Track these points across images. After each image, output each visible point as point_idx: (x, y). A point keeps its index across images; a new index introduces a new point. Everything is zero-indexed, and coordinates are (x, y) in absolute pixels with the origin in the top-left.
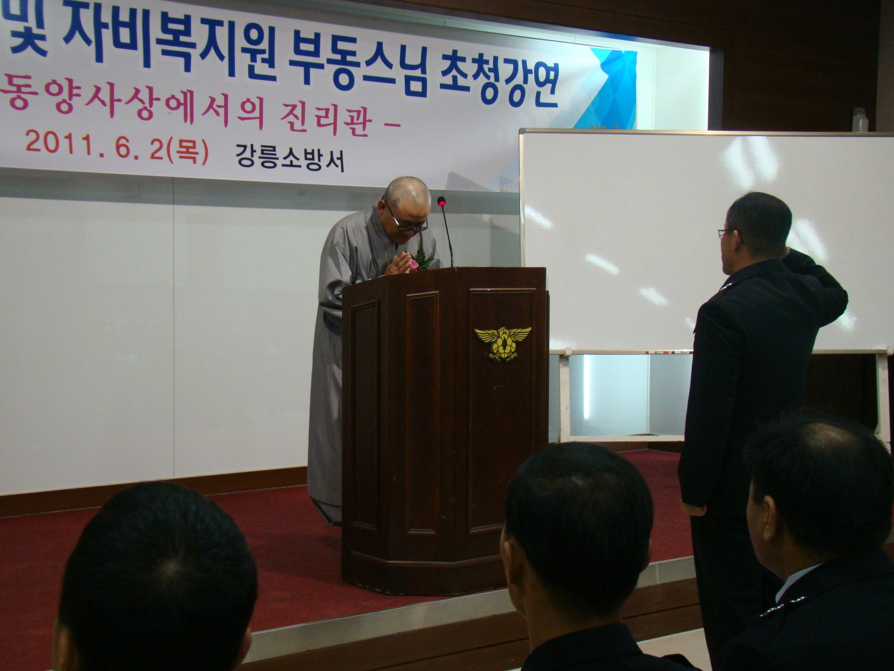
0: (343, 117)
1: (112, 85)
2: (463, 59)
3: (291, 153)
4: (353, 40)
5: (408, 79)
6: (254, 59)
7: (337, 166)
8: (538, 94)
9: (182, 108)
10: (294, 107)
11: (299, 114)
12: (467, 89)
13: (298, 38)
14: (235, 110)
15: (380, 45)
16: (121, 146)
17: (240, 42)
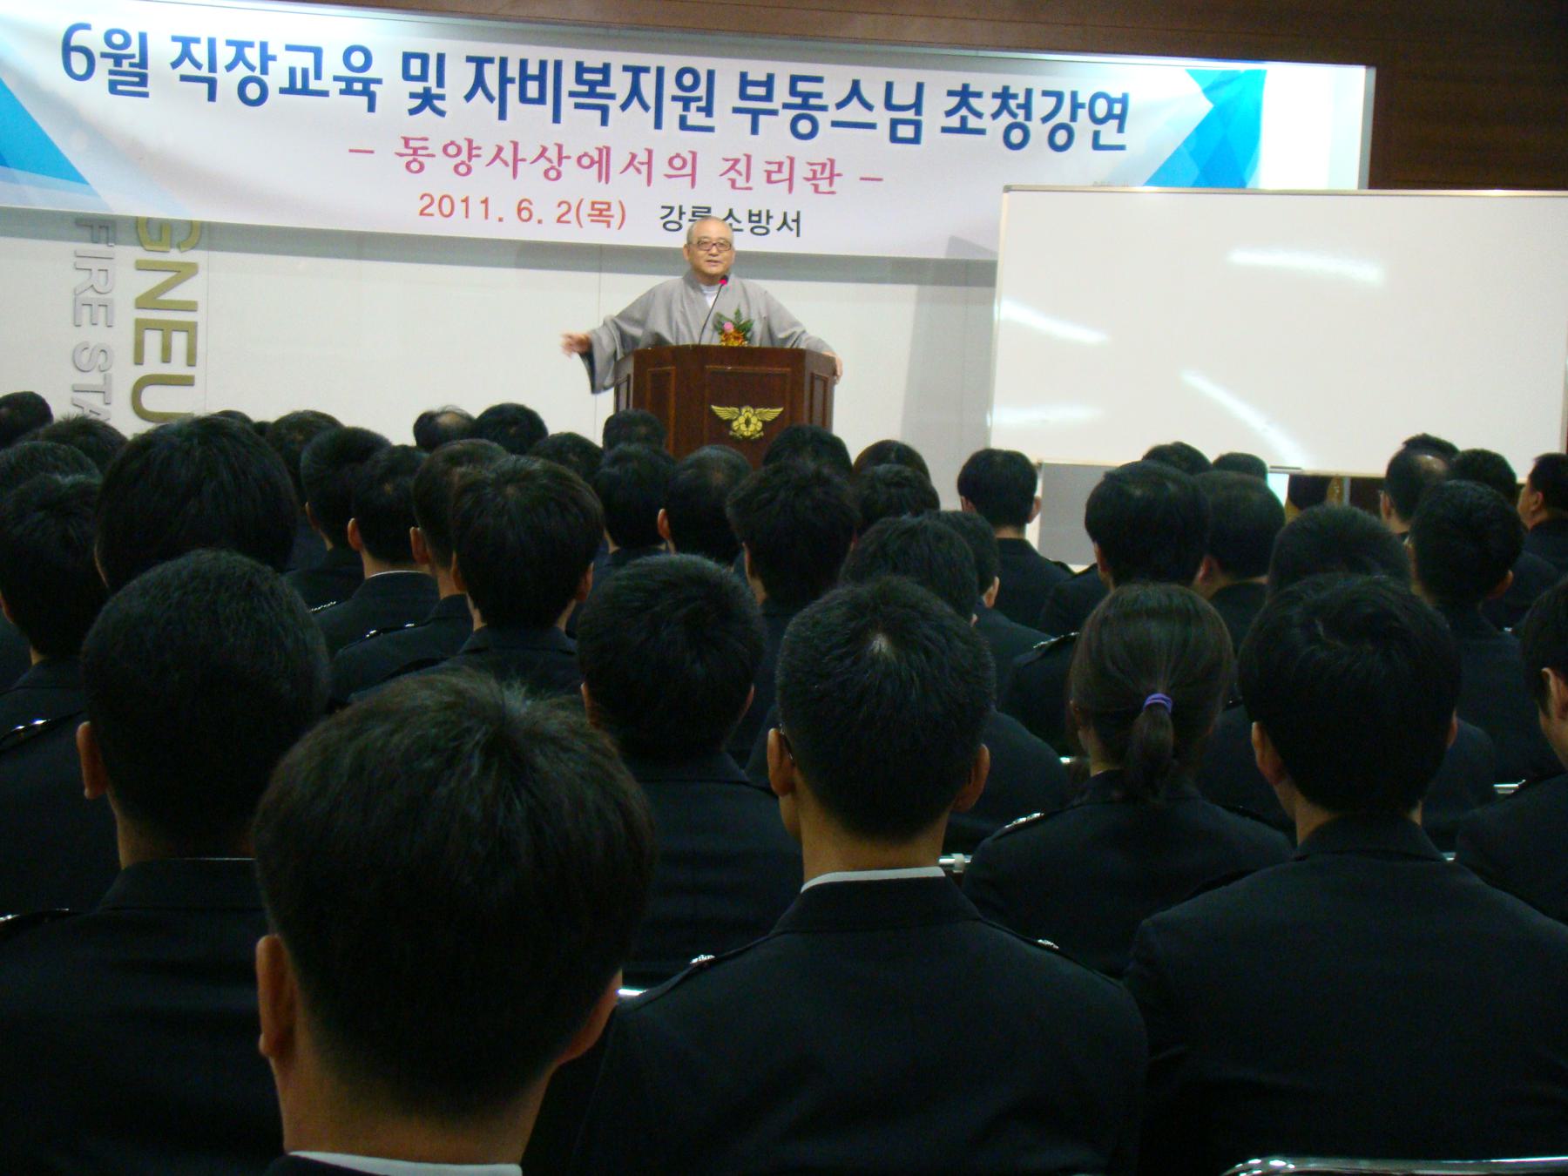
0: (802, 171)
1: (515, 145)
2: (978, 95)
3: (731, 214)
4: (819, 80)
5: (894, 123)
6: (686, 108)
7: (791, 229)
8: (1096, 135)
9: (596, 166)
10: (736, 161)
11: (743, 170)
12: (981, 132)
13: (744, 81)
14: (660, 166)
15: (856, 84)
16: (523, 209)
17: (670, 89)
